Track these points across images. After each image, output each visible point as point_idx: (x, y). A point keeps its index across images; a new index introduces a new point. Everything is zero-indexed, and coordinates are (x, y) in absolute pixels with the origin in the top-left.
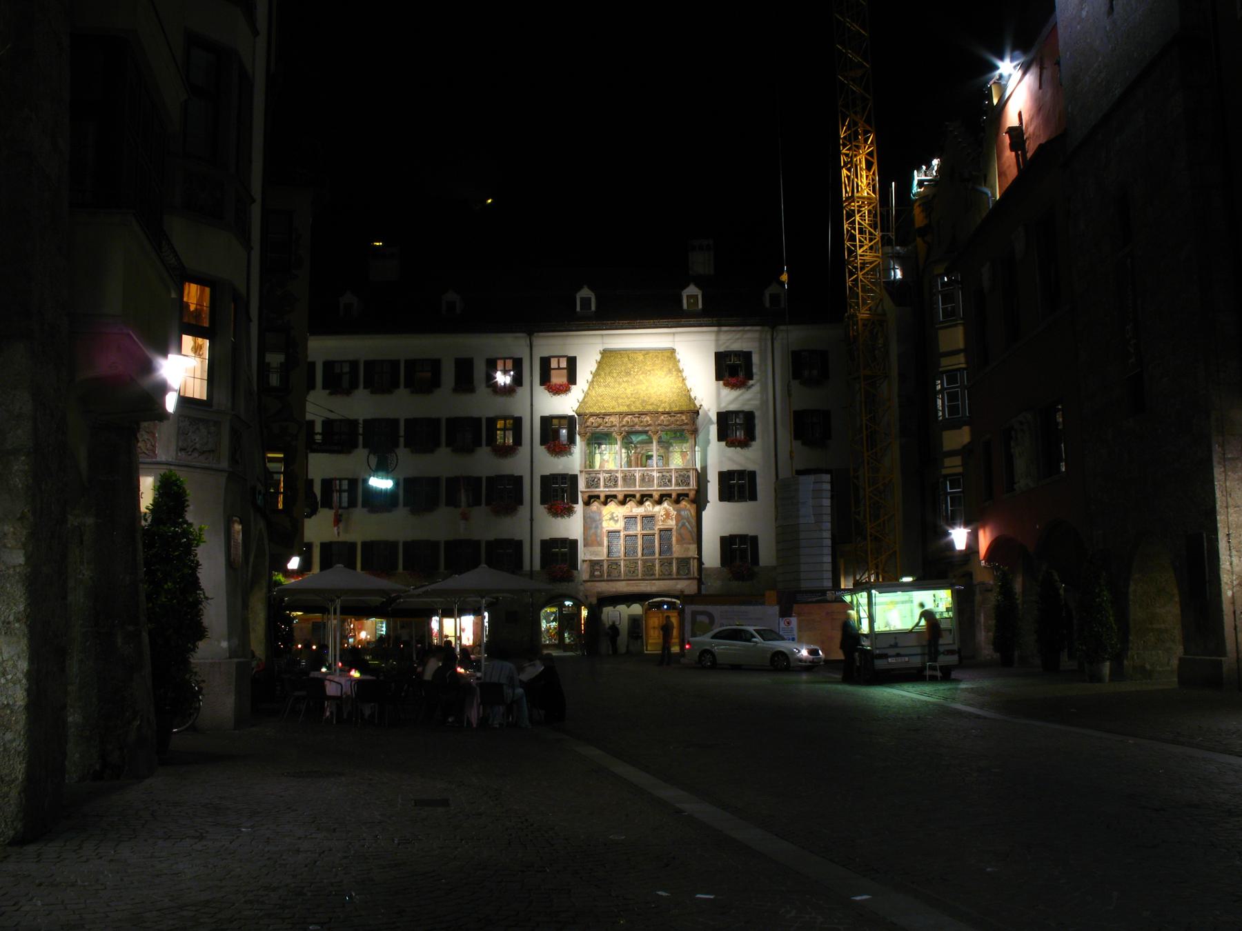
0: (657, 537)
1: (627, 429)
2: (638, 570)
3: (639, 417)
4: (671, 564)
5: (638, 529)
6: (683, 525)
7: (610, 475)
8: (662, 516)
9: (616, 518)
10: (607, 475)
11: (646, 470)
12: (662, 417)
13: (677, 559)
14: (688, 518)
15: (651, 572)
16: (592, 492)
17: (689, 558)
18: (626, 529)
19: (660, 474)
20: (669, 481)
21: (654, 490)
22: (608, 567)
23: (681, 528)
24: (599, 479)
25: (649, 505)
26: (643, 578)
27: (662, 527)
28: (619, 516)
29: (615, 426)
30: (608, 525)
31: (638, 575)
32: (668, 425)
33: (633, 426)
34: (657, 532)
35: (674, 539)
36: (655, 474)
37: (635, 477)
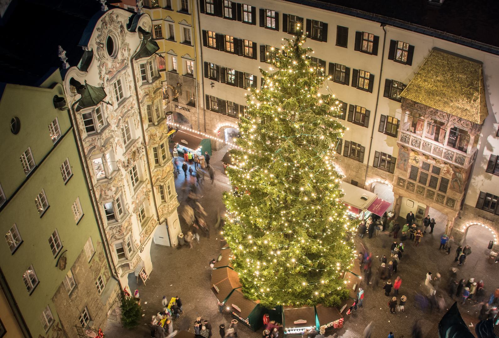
0: (439, 181)
5: (430, 173)
6: (456, 181)
9: (417, 161)
10: (414, 138)
23: (454, 181)
24: (409, 139)
27: (443, 177)
28: (419, 160)
30: (411, 162)
35: (449, 186)
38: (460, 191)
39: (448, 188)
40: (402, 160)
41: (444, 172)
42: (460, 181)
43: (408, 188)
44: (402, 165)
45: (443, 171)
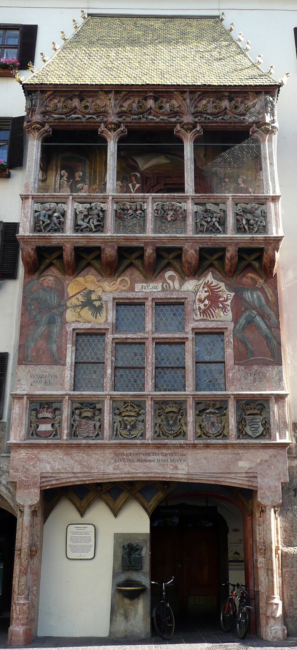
1: (128, 120)
2: (143, 421)
3: (156, 100)
7: (88, 206)
8: (201, 301)
9: (97, 304)
10: (81, 207)
11: (167, 198)
12: (204, 102)
13: (238, 399)
14: (261, 306)
15: (176, 429)
16: (44, 238)
17: (267, 398)
18: (116, 327)
20: (219, 222)
22: (73, 413)
23: (244, 328)
24: (64, 214)
25: (171, 278)
27: (202, 325)
28: (104, 298)
29: (105, 113)
31: (143, 435)
33: (142, 113)
34: (190, 336)
36: (190, 207)
37: (144, 211)
38: (273, 356)
39: (230, 361)
40: (37, 324)
41: (202, 306)
42: (263, 317)
43: (73, 434)
44: (41, 343)
45: (198, 305)
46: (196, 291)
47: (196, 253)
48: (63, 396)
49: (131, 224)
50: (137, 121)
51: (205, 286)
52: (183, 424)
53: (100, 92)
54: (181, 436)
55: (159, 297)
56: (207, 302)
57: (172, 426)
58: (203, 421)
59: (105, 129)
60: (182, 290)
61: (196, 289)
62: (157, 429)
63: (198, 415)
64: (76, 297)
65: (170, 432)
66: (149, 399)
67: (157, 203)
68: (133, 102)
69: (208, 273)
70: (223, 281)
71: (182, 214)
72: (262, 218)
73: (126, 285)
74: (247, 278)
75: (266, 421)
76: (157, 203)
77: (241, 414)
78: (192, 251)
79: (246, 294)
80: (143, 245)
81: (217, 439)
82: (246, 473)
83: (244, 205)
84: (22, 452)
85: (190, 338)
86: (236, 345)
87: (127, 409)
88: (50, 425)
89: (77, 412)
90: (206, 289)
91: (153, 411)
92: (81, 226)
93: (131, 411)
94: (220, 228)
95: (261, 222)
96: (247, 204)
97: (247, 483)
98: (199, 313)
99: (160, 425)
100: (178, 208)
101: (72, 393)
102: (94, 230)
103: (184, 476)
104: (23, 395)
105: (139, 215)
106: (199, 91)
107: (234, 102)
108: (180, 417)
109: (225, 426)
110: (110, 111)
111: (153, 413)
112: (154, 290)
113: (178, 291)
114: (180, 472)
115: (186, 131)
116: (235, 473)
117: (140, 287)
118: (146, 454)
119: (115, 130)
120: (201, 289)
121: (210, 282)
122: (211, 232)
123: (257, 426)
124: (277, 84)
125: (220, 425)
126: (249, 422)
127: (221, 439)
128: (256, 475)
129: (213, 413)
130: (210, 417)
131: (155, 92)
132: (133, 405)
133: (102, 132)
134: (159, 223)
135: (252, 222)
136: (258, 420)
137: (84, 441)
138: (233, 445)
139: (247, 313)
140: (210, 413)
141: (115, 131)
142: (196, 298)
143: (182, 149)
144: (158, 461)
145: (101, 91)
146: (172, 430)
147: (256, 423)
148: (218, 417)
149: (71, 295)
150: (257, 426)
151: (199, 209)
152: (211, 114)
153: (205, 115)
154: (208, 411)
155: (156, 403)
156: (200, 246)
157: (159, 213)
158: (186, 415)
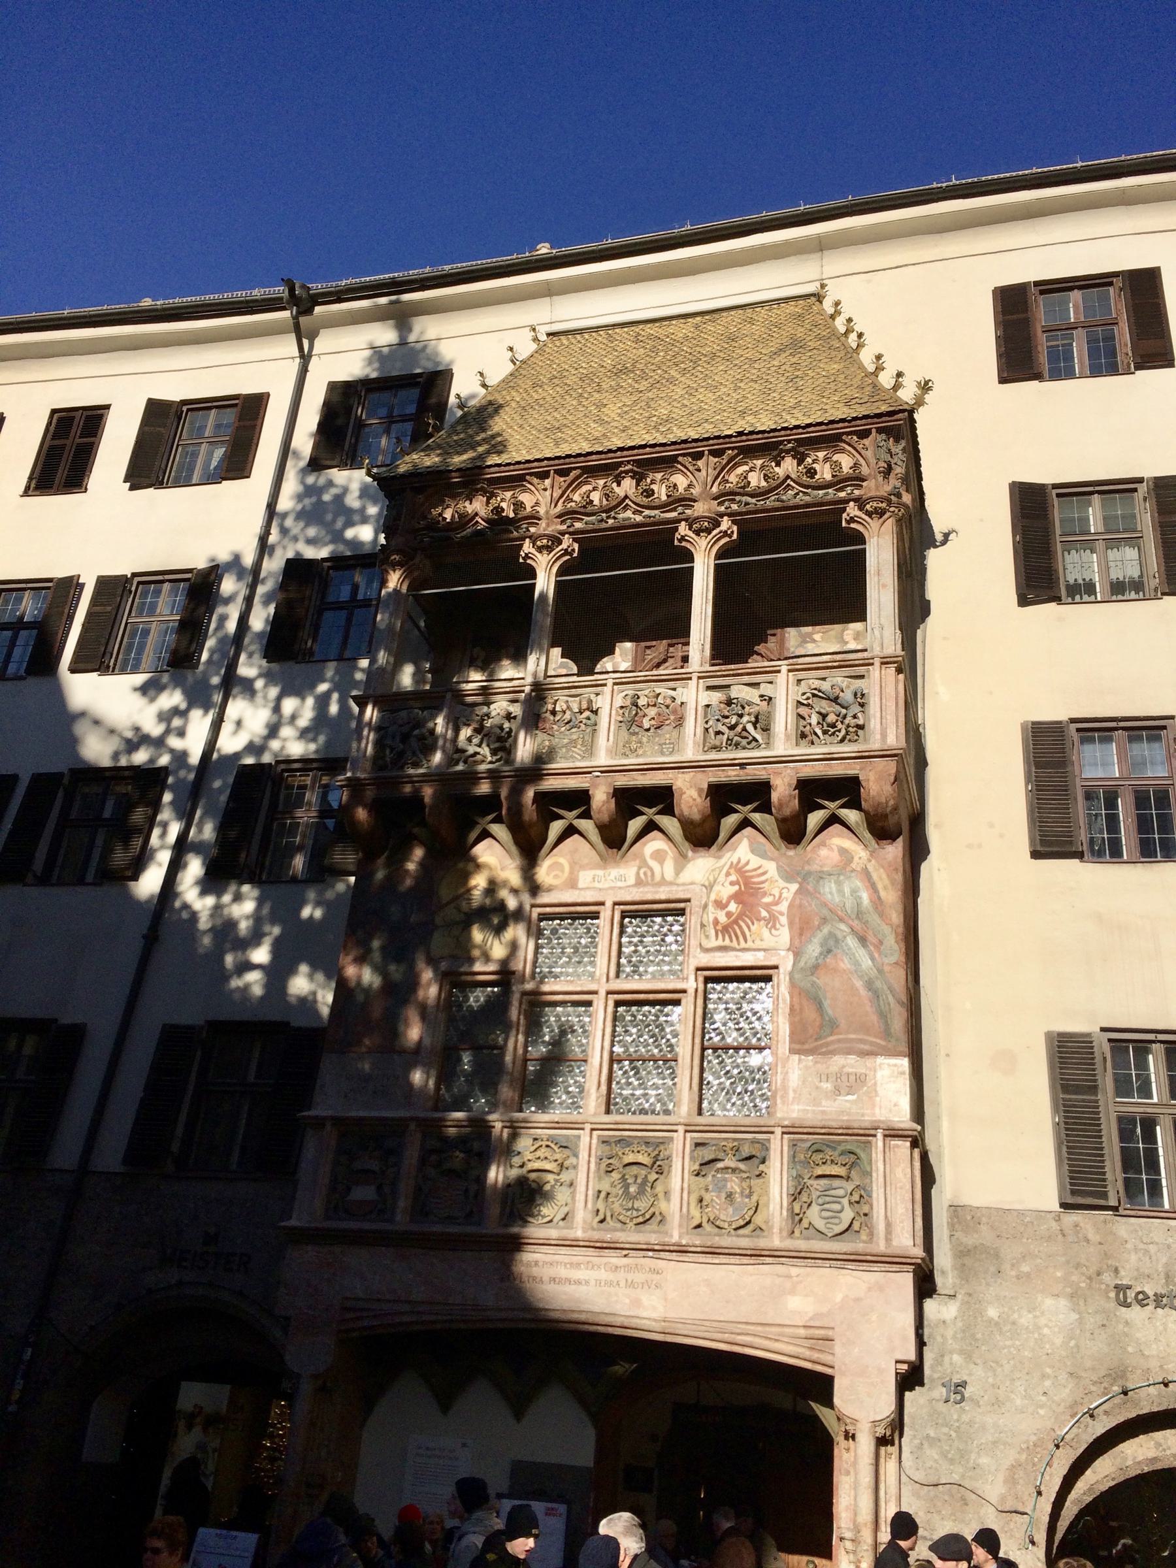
1: (578, 525)
2: (571, 1184)
3: (639, 478)
4: (756, 1159)
8: (720, 905)
14: (859, 914)
17: (865, 1134)
19: (716, 697)
21: (680, 767)
22: (423, 1161)
25: (659, 856)
26: (596, 1235)
32: (758, 494)
34: (691, 984)
37: (596, 712)
42: (863, 940)
45: (712, 913)
46: (710, 883)
47: (700, 796)
48: (403, 1123)
49: (566, 741)
50: (596, 527)
51: (732, 871)
52: (661, 1195)
53: (528, 477)
54: (653, 1225)
55: (628, 898)
56: (733, 907)
57: (635, 1197)
58: (707, 1190)
59: (533, 551)
60: (681, 880)
61: (711, 878)
62: (601, 1205)
63: (697, 1175)
64: (452, 905)
65: (629, 1213)
66: (587, 1131)
67: (624, 693)
68: (595, 489)
69: (740, 841)
70: (772, 859)
71: (675, 712)
72: (856, 709)
73: (560, 874)
74: (832, 849)
75: (861, 1196)
76: (624, 693)
77: (799, 1176)
78: (694, 793)
79: (827, 884)
80: (587, 785)
81: (738, 1236)
82: (805, 1327)
83: (817, 683)
84: (310, 1248)
85: (691, 991)
86: (797, 1007)
87: (538, 1154)
88: (373, 1188)
89: (434, 1157)
90: (733, 878)
91: (593, 1160)
92: (464, 751)
93: (546, 1158)
94: (758, 737)
95: (855, 717)
96: (824, 679)
97: (807, 1353)
98: (713, 932)
99: (608, 1194)
100: (668, 701)
101: (422, 1115)
102: (489, 759)
103: (654, 1323)
104: (325, 1118)
105: (584, 721)
106: (729, 448)
107: (809, 460)
108: (656, 1176)
109: (760, 1202)
110: (542, 510)
111: (593, 1166)
112: (619, 884)
113: (671, 884)
114: (645, 1314)
115: (697, 533)
116: (780, 1325)
117: (590, 879)
118: (571, 1264)
119: (549, 549)
120: (722, 878)
121: (743, 862)
122: (737, 745)
123: (837, 1207)
124: (906, 407)
125: (747, 1200)
126: (819, 1197)
127: (748, 1236)
128: (830, 1333)
129: (734, 1170)
130: (725, 1180)
131: (638, 463)
132: (552, 1145)
133: (527, 556)
134: (624, 734)
135: (831, 718)
136: (841, 1192)
137: (437, 1228)
138: (775, 1255)
139: (826, 930)
140: (727, 1168)
141: (550, 552)
142: (708, 897)
143: (687, 576)
144: (598, 1282)
145: (528, 474)
146: (633, 1208)
147: (837, 1199)
148: (744, 1179)
149: (445, 900)
150: (837, 1207)
151: (714, 699)
152: (752, 496)
153: (738, 498)
154: (720, 1165)
155: (604, 1142)
156: (711, 780)
157: (626, 715)
158: (669, 1172)
